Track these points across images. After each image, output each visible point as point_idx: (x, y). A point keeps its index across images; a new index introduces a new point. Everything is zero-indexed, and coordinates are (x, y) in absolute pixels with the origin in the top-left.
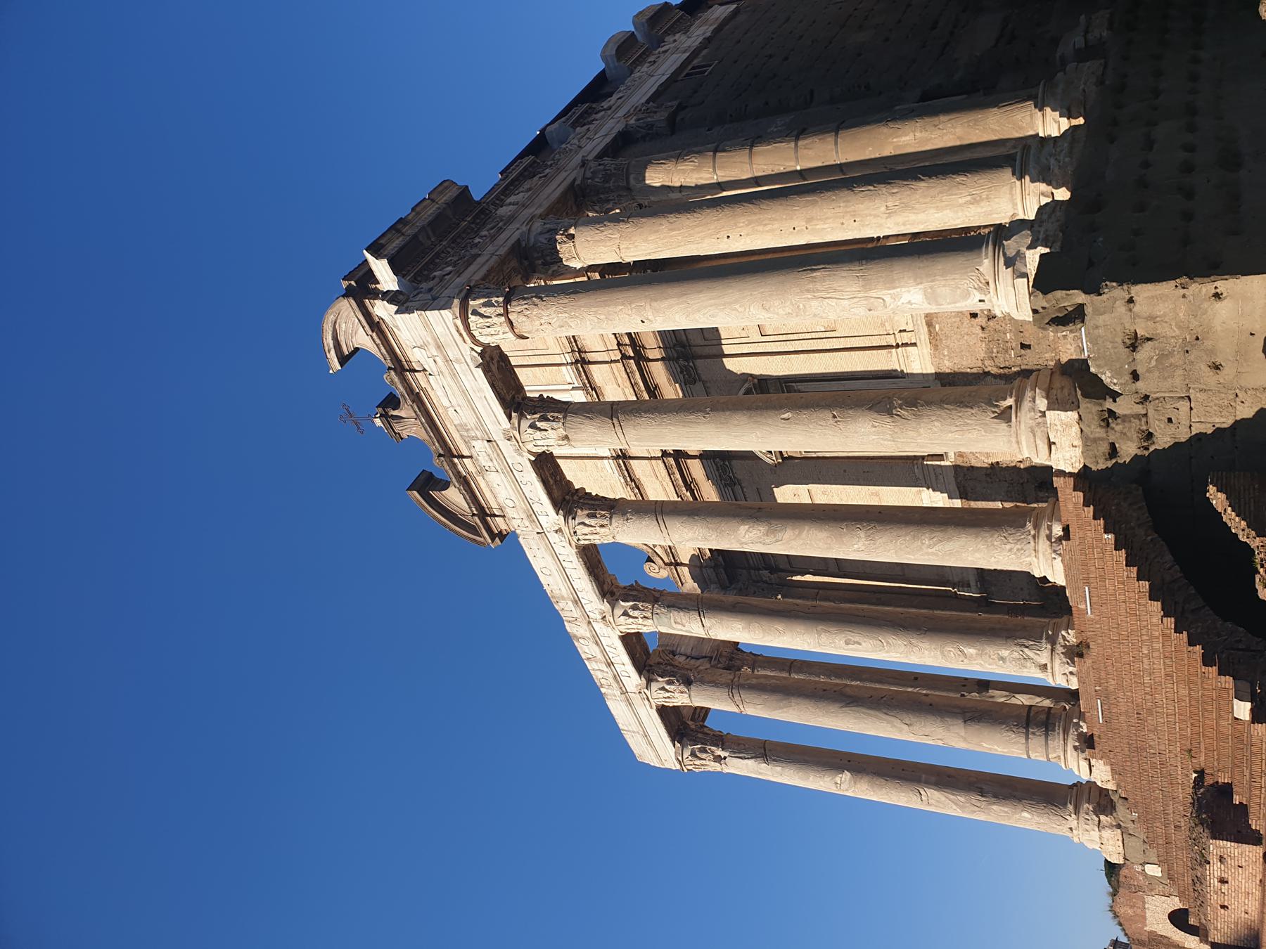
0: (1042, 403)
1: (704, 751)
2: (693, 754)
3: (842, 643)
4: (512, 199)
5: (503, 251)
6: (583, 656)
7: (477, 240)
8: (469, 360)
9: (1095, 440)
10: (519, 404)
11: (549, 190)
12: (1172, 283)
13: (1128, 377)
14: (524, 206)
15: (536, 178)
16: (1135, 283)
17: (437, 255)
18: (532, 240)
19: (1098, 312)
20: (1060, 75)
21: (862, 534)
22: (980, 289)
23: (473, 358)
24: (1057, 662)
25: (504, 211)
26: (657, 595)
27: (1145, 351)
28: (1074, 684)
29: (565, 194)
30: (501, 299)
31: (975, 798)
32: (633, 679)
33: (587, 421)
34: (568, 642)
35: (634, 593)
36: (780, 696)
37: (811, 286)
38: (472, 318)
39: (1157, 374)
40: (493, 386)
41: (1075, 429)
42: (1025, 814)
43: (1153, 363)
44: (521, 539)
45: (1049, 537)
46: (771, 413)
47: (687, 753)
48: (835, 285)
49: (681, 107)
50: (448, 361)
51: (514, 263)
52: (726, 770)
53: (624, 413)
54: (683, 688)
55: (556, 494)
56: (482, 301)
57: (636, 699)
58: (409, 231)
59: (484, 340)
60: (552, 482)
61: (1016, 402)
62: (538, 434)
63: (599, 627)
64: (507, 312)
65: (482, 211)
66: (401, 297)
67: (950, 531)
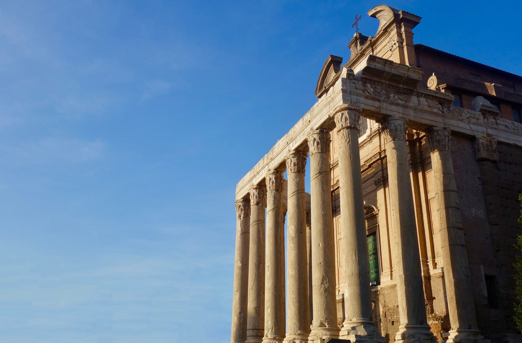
2: (240, 206)
4: (423, 100)
5: (383, 112)
7: (392, 95)
11: (427, 116)
14: (415, 109)
15: (440, 106)
17: (380, 82)
18: (392, 122)
20: (482, 337)
21: (293, 273)
25: (414, 100)
26: (280, 190)
29: (425, 125)
30: (349, 125)
33: (318, 163)
34: (261, 156)
36: (256, 240)
37: (350, 255)
38: (340, 114)
40: (325, 122)
44: (286, 135)
46: (322, 239)
48: (350, 265)
49: (494, 162)
50: (329, 103)
51: (380, 117)
54: (255, 202)
56: (348, 117)
57: (250, 184)
58: (387, 69)
62: (312, 142)
64: (343, 128)
65: (411, 90)
66: (351, 77)
67: (297, 304)
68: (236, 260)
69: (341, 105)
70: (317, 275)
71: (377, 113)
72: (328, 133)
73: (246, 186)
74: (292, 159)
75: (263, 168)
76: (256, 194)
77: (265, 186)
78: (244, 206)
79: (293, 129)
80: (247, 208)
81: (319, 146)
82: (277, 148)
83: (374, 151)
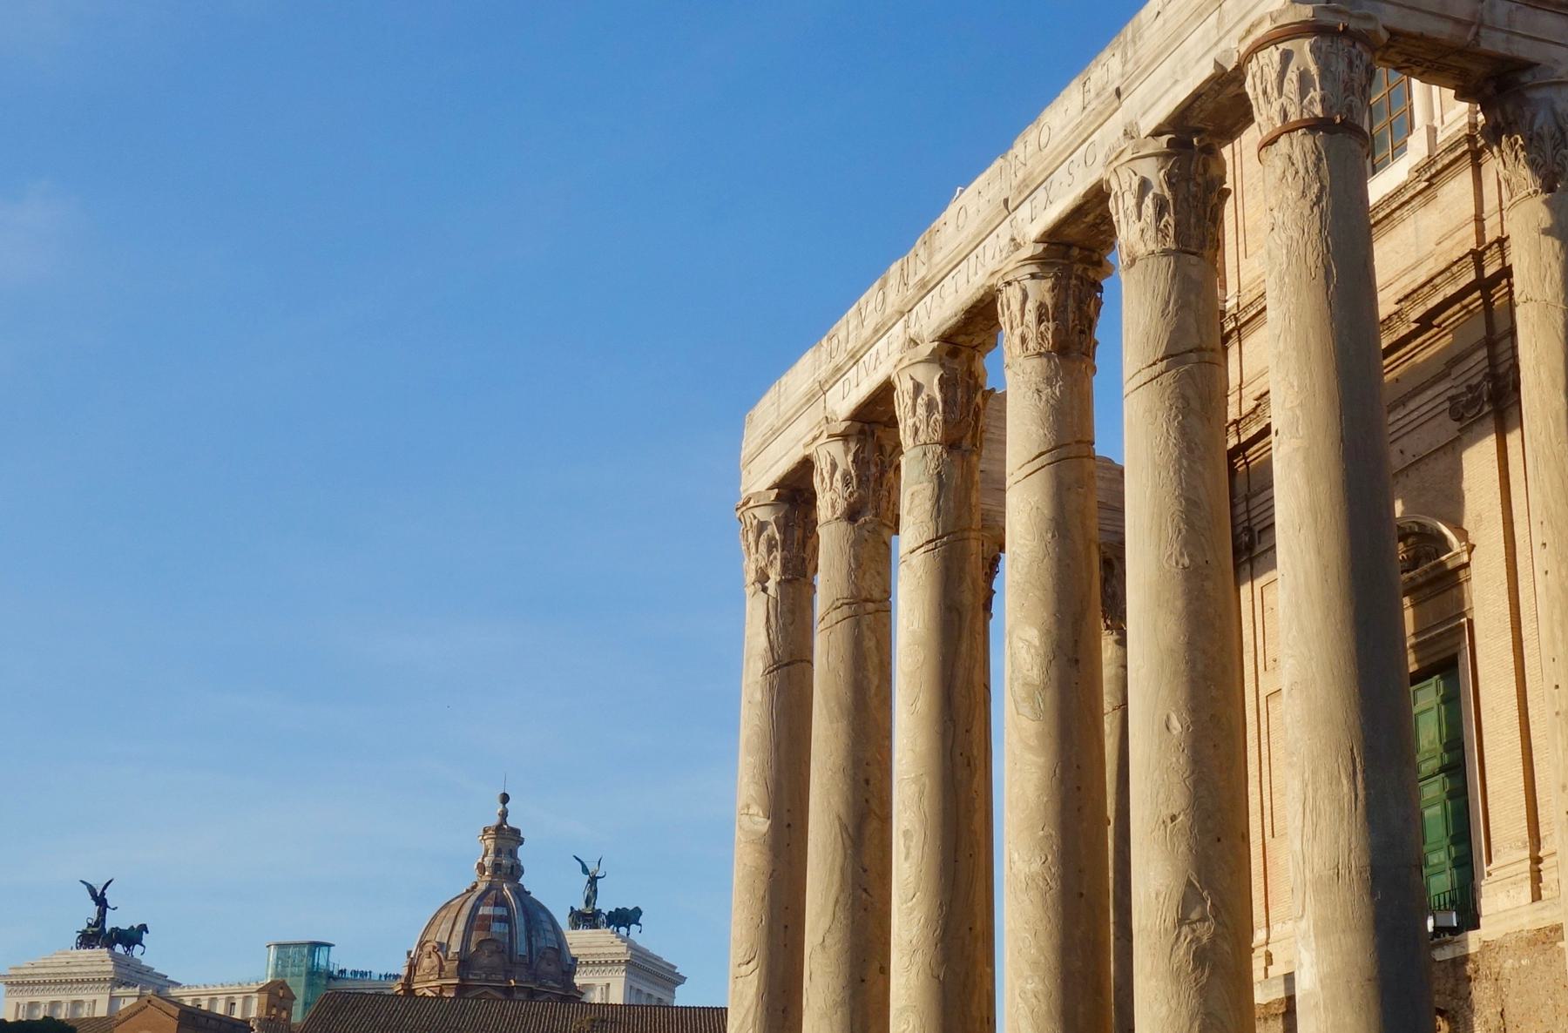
1: (771, 547)
2: (762, 526)
6: (863, 300)
21: (1036, 866)
26: (966, 444)
30: (1318, 110)
33: (1159, 305)
36: (847, 697)
37: (1323, 776)
38: (1272, 55)
40: (1196, 96)
44: (999, 162)
46: (1181, 695)
51: (1478, 70)
52: (749, 590)
53: (1179, 380)
54: (841, 506)
56: (1313, 69)
60: (1090, 218)
62: (1130, 201)
64: (1289, 130)
68: (740, 803)
69: (1281, 12)
70: (1154, 877)
71: (1461, 52)
72: (1211, 152)
73: (793, 421)
74: (1030, 285)
75: (880, 331)
76: (845, 462)
77: (893, 423)
78: (785, 525)
79: (1031, 135)
80: (798, 533)
81: (1169, 218)
82: (951, 228)
83: (1447, 245)
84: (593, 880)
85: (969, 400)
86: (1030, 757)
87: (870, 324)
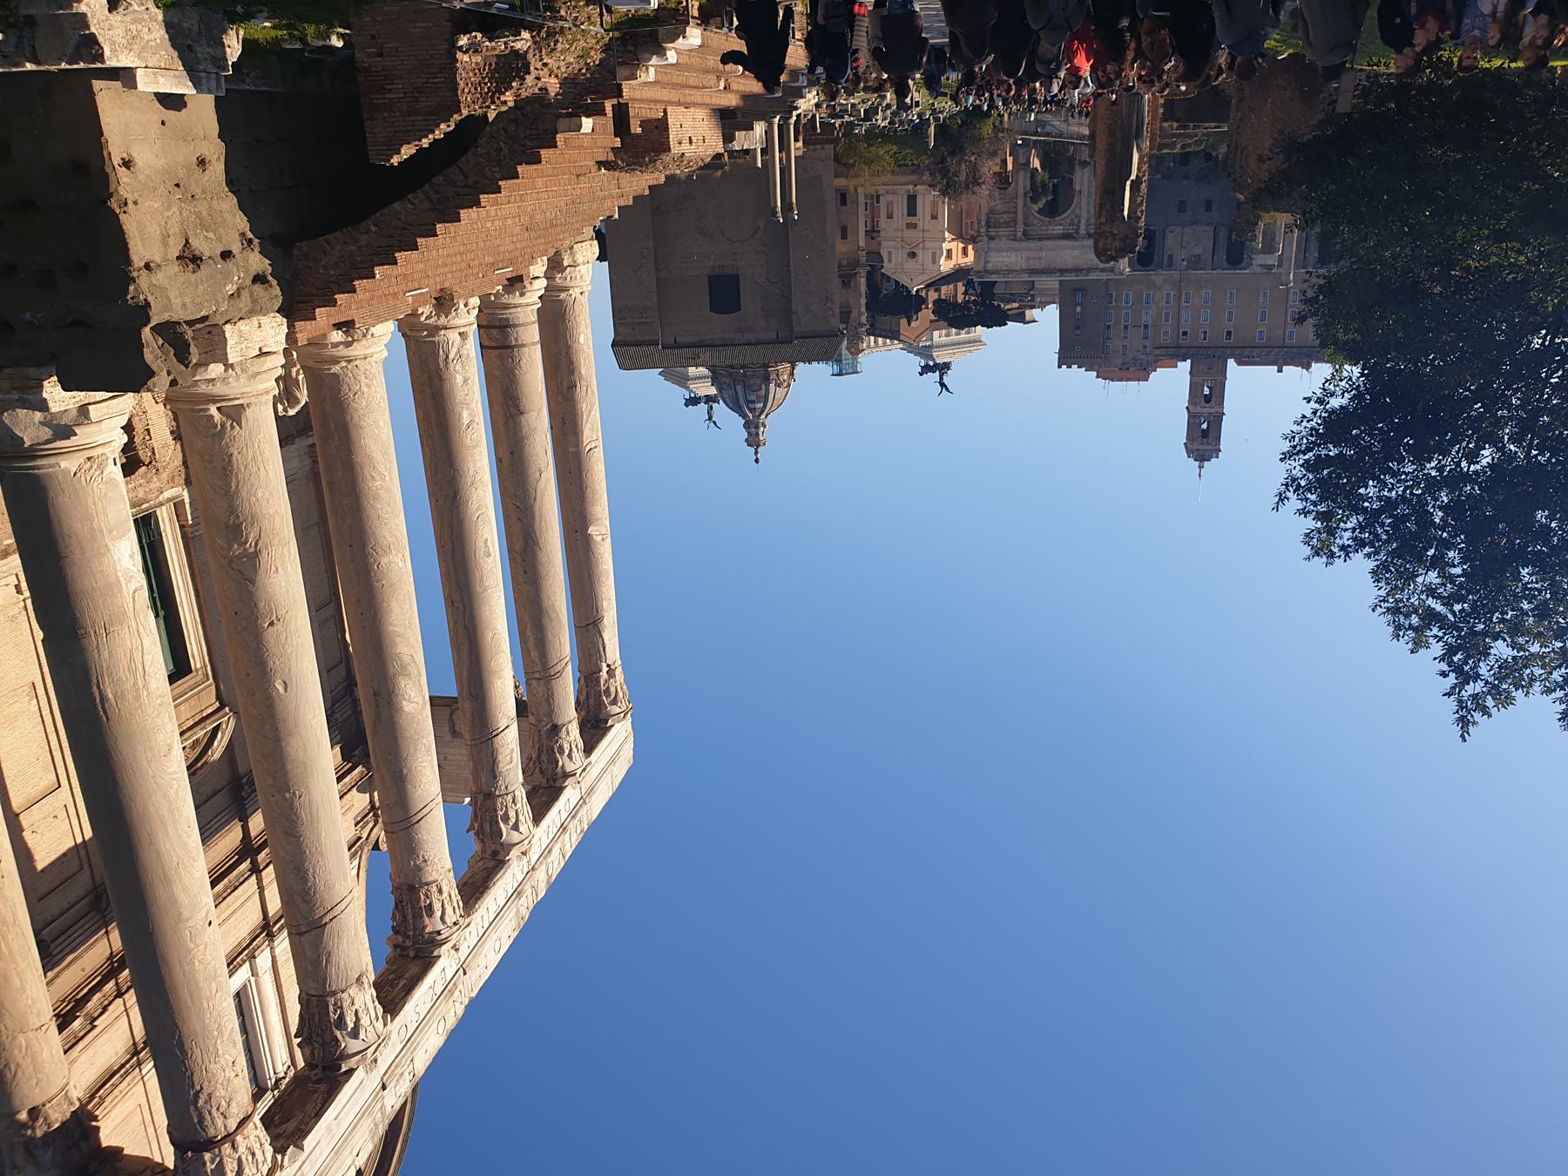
0: (216, 370)
2: (614, 702)
3: (490, 560)
8: (298, 1164)
9: (254, 301)
10: (324, 1069)
12: (122, 217)
13: (230, 264)
16: (129, 262)
19: (168, 306)
21: (384, 561)
22: (101, 467)
23: (292, 1161)
24: (457, 322)
26: (480, 798)
27: (201, 245)
28: (475, 301)
30: (207, 1156)
31: (580, 392)
32: (570, 795)
33: (334, 959)
35: (487, 826)
36: (546, 620)
39: (221, 230)
40: (319, 1115)
41: (242, 325)
42: (582, 340)
43: (211, 235)
44: (473, 995)
45: (348, 345)
47: (615, 709)
52: (619, 662)
53: (312, 911)
54: (563, 734)
55: (414, 969)
59: (269, 1156)
61: (214, 402)
62: (365, 1021)
63: (534, 855)
64: (229, 1137)
67: (359, 458)
68: (609, 540)
73: (600, 773)
74: (440, 926)
75: (547, 851)
76: (563, 761)
77: (530, 796)
79: (451, 1022)
81: (334, 1017)
84: (710, 418)
85: (481, 825)
86: (399, 629)
87: (556, 851)
